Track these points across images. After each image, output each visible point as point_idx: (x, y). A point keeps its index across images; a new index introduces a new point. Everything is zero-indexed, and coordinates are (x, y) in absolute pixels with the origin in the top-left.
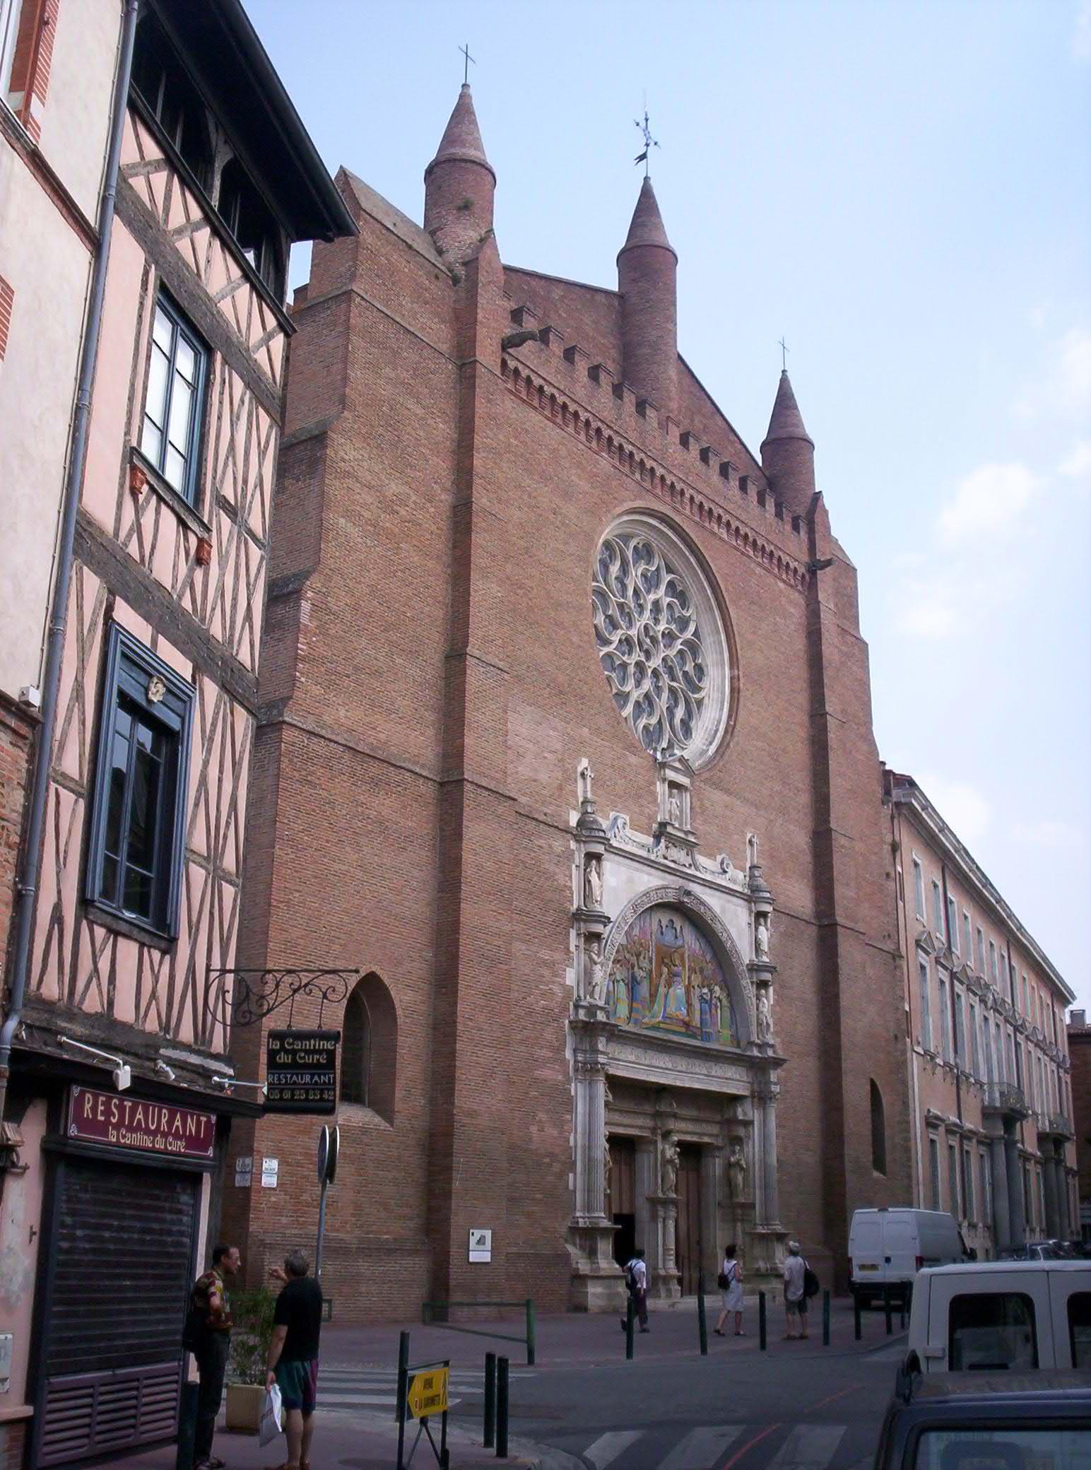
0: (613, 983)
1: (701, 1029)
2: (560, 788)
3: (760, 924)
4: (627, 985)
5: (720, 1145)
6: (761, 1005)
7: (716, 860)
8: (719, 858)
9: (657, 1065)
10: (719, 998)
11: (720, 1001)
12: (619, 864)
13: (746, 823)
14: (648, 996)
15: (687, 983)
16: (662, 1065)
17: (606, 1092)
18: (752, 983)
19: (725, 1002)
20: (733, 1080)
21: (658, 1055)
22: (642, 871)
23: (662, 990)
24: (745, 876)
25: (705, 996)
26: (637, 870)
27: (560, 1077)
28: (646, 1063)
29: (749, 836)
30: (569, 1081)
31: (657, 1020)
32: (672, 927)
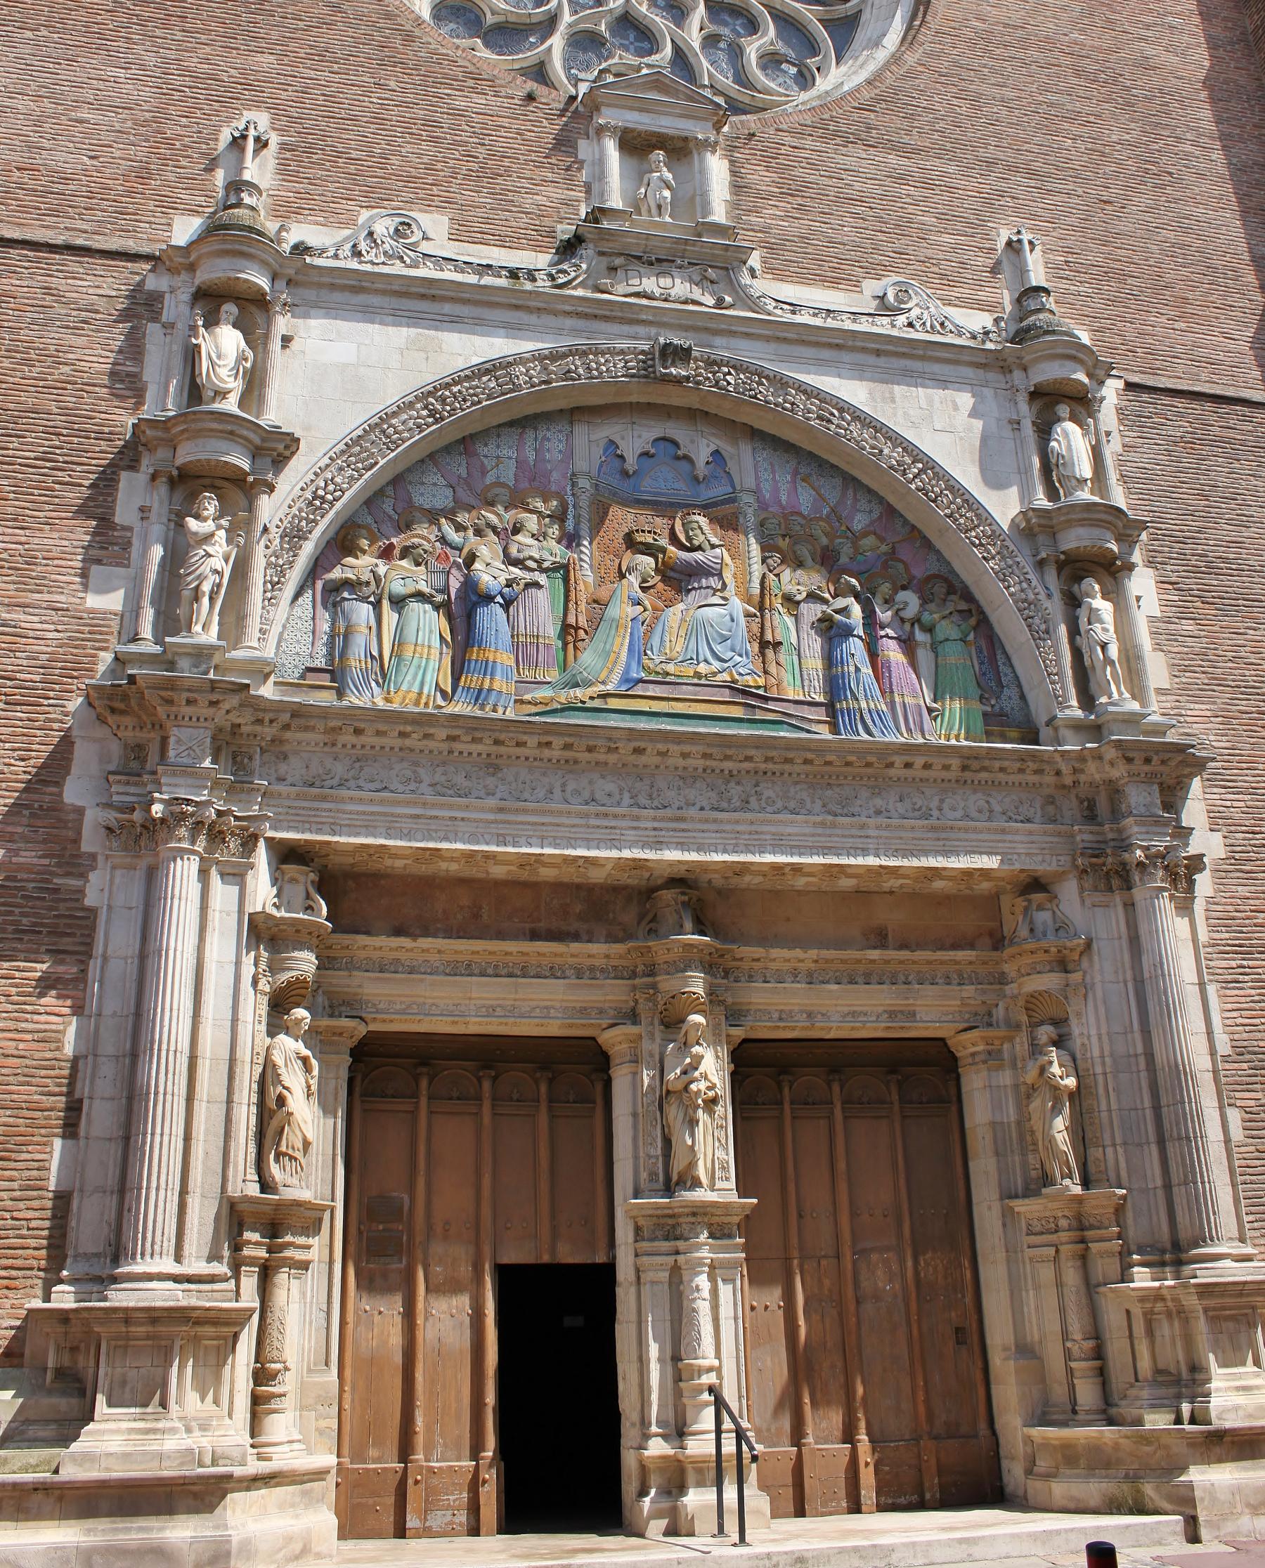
0: (377, 606)
3: (1059, 420)
4: (443, 607)
10: (916, 621)
11: (930, 630)
13: (990, 202)
14: (551, 630)
17: (308, 896)
18: (1041, 564)
19: (946, 629)
23: (621, 610)
24: (997, 321)
27: (28, 857)
29: (1004, 235)
30: (78, 864)
32: (678, 458)
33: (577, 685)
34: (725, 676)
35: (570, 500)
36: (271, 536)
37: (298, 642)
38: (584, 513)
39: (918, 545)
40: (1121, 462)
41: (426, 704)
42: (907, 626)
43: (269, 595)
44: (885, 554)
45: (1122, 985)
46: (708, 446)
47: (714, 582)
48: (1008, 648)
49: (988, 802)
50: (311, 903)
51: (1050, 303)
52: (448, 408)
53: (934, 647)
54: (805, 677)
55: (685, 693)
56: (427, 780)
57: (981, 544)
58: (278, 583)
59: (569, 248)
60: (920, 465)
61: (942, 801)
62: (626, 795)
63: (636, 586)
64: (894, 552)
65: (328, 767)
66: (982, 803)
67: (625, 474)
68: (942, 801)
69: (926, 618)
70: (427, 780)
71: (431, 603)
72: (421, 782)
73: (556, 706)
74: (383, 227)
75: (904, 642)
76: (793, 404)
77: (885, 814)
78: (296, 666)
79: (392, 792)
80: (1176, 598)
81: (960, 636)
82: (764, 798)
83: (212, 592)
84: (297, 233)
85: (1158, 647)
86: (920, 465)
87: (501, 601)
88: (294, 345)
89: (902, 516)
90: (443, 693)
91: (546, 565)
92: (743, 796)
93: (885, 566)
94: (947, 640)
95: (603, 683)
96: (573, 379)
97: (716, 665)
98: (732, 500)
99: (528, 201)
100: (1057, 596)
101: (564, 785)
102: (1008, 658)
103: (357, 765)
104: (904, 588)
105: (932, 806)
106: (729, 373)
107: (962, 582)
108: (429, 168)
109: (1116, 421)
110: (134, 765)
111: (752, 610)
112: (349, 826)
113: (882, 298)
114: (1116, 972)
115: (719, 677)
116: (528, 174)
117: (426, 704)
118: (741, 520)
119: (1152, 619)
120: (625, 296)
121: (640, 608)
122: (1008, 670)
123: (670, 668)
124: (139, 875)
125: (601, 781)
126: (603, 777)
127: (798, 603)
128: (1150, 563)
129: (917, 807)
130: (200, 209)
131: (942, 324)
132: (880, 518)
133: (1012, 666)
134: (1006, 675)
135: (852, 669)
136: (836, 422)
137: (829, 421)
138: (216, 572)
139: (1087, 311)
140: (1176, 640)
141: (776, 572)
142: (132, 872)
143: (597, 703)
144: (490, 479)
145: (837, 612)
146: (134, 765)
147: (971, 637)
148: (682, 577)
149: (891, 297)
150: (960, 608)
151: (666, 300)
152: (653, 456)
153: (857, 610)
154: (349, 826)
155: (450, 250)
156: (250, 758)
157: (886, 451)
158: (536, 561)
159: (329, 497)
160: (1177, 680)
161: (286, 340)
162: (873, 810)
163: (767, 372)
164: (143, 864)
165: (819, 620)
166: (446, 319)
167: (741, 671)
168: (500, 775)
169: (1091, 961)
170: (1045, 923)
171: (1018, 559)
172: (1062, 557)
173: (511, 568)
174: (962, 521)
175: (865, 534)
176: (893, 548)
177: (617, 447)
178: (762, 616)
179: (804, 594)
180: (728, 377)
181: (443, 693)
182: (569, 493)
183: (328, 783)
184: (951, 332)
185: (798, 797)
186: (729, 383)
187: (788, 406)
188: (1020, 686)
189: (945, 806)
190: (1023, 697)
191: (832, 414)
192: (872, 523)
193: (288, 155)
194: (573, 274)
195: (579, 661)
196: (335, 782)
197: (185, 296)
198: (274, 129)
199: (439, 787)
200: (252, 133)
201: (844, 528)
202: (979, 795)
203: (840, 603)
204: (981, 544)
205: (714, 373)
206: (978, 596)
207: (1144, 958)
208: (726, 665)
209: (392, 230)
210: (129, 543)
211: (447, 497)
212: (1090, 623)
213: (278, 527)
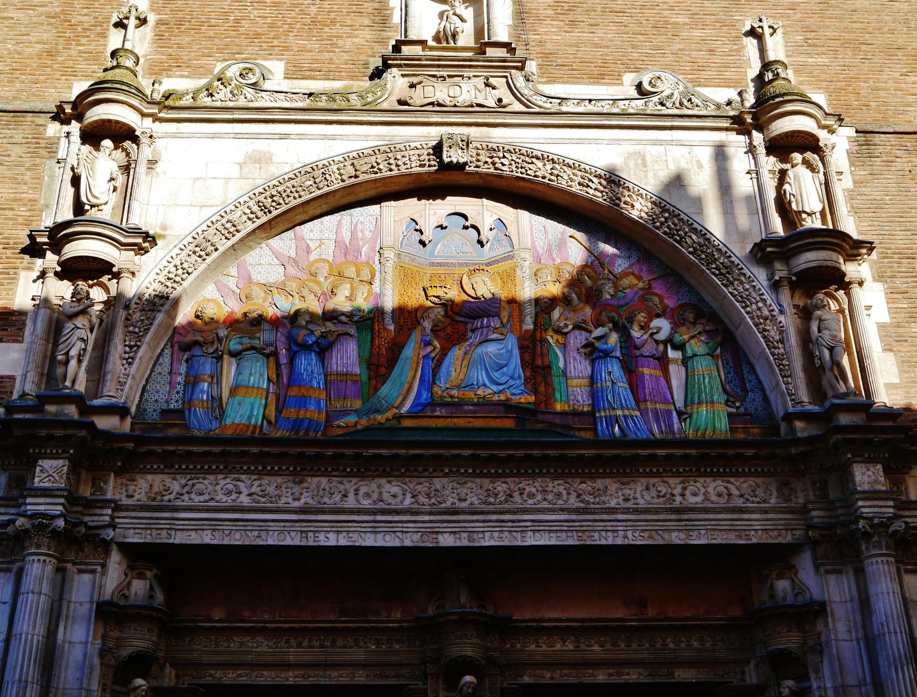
1: (592, 414)
2: (51, 54)
5: (755, 681)
6: (814, 327)
7: (622, 84)
8: (629, 79)
9: (351, 502)
10: (669, 341)
11: (680, 347)
12: (214, 136)
15: (529, 325)
16: (366, 503)
17: (152, 588)
18: (775, 286)
19: (696, 347)
20: (706, 511)
21: (350, 485)
22: (302, 136)
25: (597, 344)
26: (284, 137)
28: (296, 504)
31: (389, 414)
32: (466, 228)
33: (377, 411)
34: (503, 398)
35: (377, 266)
36: (131, 312)
37: (158, 392)
38: (389, 278)
39: (671, 280)
40: (851, 196)
41: (253, 432)
42: (661, 347)
43: (127, 356)
44: (641, 289)
45: (855, 642)
46: (492, 216)
47: (494, 322)
48: (751, 357)
49: (726, 488)
50: (153, 593)
51: (790, 74)
52: (274, 204)
53: (685, 361)
54: (570, 393)
55: (466, 412)
56: (245, 491)
57: (721, 274)
58: (133, 346)
59: (377, 74)
60: (667, 215)
61: (684, 489)
62: (409, 495)
63: (428, 331)
64: (650, 288)
65: (168, 485)
66: (721, 489)
67: (422, 243)
68: (684, 489)
69: (678, 338)
70: (245, 491)
71: (262, 354)
72: (240, 493)
73: (359, 427)
74: (233, 71)
75: (658, 359)
76: (558, 175)
77: (632, 501)
78: (155, 410)
79: (217, 502)
80: (905, 306)
81: (707, 350)
82: (526, 492)
83: (79, 355)
84: (169, 84)
85: (887, 349)
86: (667, 215)
87: (317, 349)
88: (159, 167)
89: (657, 258)
90: (269, 422)
91: (355, 319)
92: (508, 492)
93: (643, 299)
94: (695, 355)
95: (397, 408)
96: (376, 173)
97: (495, 388)
98: (509, 257)
99: (348, 43)
100: (789, 310)
101: (357, 490)
102: (752, 367)
103: (190, 483)
104: (658, 316)
105: (675, 492)
106: (504, 157)
107: (711, 307)
108: (272, 26)
109: (847, 163)
110: (15, 493)
111: (526, 343)
112: (183, 530)
113: (639, 86)
114: (849, 631)
115: (496, 398)
116: (349, 23)
117: (253, 432)
118: (518, 272)
119: (881, 327)
120: (422, 106)
121: (429, 349)
122: (752, 378)
123: (454, 392)
124: (12, 576)
125: (388, 486)
126: (389, 482)
127: (566, 334)
128: (879, 277)
129: (661, 494)
130: (95, 75)
131: (690, 100)
132: (638, 261)
133: (755, 373)
134: (750, 381)
135: (609, 384)
136: (593, 186)
137: (588, 186)
138: (83, 340)
139: (823, 76)
140: (906, 341)
141: (548, 311)
142: (8, 575)
143: (394, 423)
144: (313, 257)
145: (598, 339)
146: (15, 493)
147: (719, 351)
148: (468, 320)
149: (646, 85)
150: (707, 328)
151: (455, 106)
152: (446, 228)
153: (614, 338)
154: (183, 530)
155: (285, 86)
156: (106, 483)
157: (637, 205)
158: (347, 316)
159: (178, 279)
160: (907, 375)
161: (152, 163)
162: (622, 498)
163: (535, 153)
164: (16, 567)
165: (584, 347)
166: (277, 137)
167: (515, 391)
168: (305, 485)
169: (826, 624)
170: (784, 590)
171: (754, 284)
172: (794, 278)
173: (329, 324)
174: (703, 256)
175: (625, 274)
176: (650, 284)
177: (417, 224)
178: (534, 347)
179: (571, 327)
180: (503, 160)
181: (269, 422)
182: (377, 262)
183: (166, 498)
184: (697, 106)
185: (556, 490)
186: (503, 165)
187: (552, 178)
188: (763, 389)
189: (687, 492)
190: (766, 399)
191: (590, 180)
192: (631, 266)
193: (163, 28)
194: (379, 93)
195: (379, 393)
196: (172, 497)
197: (76, 138)
198: (152, 10)
199: (255, 496)
200: (134, 12)
201: (606, 271)
202: (719, 482)
203: (598, 332)
204: (721, 274)
205: (491, 157)
206: (725, 319)
207: (874, 618)
208: (501, 388)
209: (238, 73)
210: (24, 324)
211: (279, 273)
212: (819, 331)
213: (136, 303)
